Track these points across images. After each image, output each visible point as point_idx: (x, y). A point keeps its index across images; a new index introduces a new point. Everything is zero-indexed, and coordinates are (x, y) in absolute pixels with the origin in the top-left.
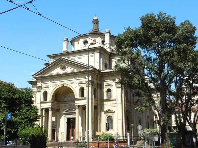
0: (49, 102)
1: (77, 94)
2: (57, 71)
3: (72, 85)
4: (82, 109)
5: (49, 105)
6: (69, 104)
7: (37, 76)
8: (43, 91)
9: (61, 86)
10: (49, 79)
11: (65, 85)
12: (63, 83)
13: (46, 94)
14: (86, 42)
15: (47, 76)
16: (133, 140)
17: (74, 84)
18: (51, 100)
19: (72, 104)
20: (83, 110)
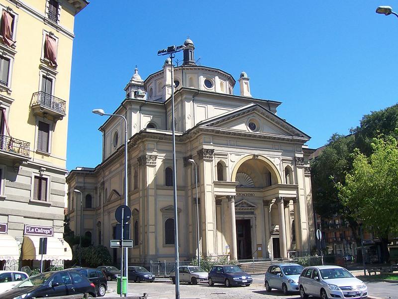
0: (230, 185)
1: (282, 179)
2: (243, 127)
3: (272, 160)
4: (263, 206)
5: (232, 192)
6: (240, 192)
7: (210, 128)
8: (216, 160)
9: (251, 157)
10: (236, 140)
11: (260, 158)
12: (256, 152)
13: (221, 167)
14: (209, 83)
15: (224, 133)
16: (178, 260)
17: (274, 158)
18: (234, 180)
19: (244, 193)
20: (264, 205)
